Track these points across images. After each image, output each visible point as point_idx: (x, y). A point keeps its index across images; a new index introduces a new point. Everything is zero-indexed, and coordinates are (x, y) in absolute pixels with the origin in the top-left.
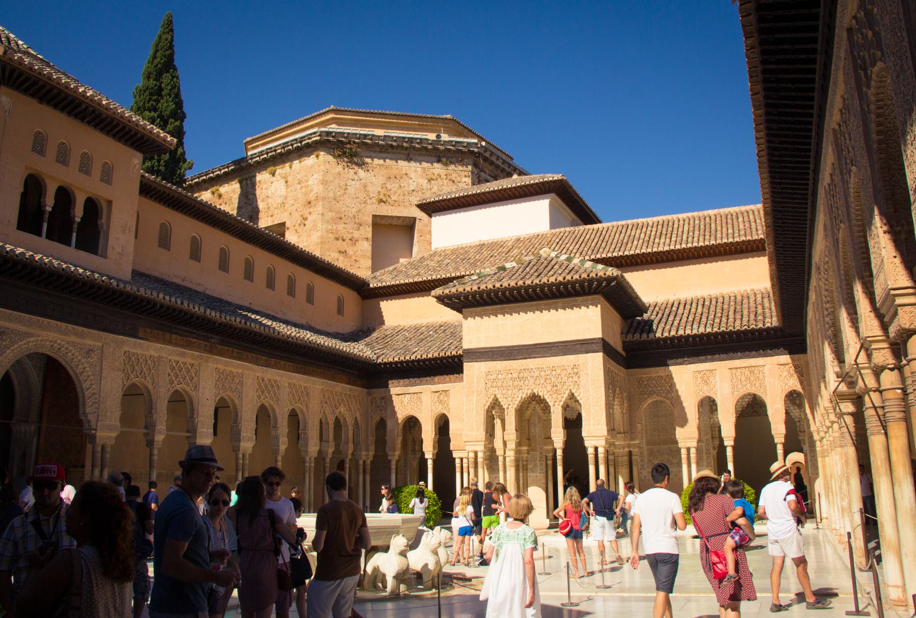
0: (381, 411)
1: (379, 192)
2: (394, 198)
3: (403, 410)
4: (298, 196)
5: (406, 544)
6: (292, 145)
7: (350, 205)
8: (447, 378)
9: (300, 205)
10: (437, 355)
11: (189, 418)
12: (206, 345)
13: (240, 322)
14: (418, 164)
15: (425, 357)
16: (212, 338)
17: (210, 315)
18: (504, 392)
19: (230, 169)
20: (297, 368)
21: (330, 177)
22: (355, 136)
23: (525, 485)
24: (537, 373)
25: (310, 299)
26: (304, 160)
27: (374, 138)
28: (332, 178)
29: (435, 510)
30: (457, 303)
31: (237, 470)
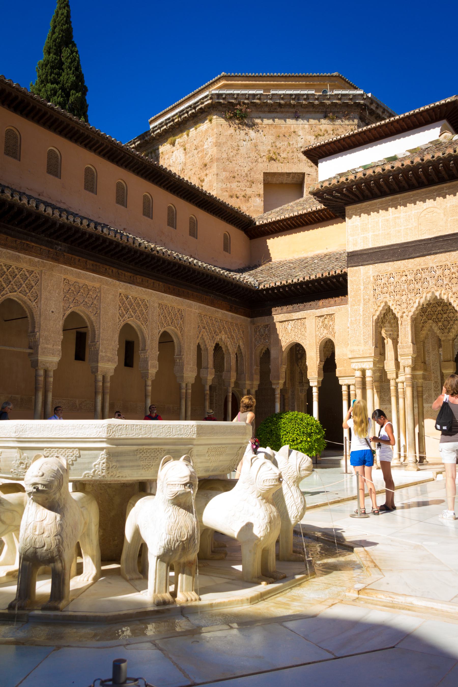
0: (264, 339)
1: (269, 151)
2: (283, 155)
3: (287, 337)
4: (196, 161)
5: (187, 480)
6: (187, 112)
7: (242, 164)
8: (332, 301)
9: (197, 169)
10: (320, 276)
11: (31, 332)
12: (49, 251)
13: (88, 225)
14: (305, 121)
15: (308, 279)
16: (58, 244)
17: (45, 211)
18: (396, 298)
19: (136, 144)
20: (169, 288)
21: (222, 139)
22: (244, 97)
23: (421, 415)
24: (439, 272)
25: (193, 232)
26: (199, 126)
27: (262, 97)
28: (224, 140)
29: (318, 439)
30: (338, 198)
31: (96, 393)
